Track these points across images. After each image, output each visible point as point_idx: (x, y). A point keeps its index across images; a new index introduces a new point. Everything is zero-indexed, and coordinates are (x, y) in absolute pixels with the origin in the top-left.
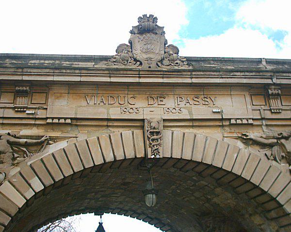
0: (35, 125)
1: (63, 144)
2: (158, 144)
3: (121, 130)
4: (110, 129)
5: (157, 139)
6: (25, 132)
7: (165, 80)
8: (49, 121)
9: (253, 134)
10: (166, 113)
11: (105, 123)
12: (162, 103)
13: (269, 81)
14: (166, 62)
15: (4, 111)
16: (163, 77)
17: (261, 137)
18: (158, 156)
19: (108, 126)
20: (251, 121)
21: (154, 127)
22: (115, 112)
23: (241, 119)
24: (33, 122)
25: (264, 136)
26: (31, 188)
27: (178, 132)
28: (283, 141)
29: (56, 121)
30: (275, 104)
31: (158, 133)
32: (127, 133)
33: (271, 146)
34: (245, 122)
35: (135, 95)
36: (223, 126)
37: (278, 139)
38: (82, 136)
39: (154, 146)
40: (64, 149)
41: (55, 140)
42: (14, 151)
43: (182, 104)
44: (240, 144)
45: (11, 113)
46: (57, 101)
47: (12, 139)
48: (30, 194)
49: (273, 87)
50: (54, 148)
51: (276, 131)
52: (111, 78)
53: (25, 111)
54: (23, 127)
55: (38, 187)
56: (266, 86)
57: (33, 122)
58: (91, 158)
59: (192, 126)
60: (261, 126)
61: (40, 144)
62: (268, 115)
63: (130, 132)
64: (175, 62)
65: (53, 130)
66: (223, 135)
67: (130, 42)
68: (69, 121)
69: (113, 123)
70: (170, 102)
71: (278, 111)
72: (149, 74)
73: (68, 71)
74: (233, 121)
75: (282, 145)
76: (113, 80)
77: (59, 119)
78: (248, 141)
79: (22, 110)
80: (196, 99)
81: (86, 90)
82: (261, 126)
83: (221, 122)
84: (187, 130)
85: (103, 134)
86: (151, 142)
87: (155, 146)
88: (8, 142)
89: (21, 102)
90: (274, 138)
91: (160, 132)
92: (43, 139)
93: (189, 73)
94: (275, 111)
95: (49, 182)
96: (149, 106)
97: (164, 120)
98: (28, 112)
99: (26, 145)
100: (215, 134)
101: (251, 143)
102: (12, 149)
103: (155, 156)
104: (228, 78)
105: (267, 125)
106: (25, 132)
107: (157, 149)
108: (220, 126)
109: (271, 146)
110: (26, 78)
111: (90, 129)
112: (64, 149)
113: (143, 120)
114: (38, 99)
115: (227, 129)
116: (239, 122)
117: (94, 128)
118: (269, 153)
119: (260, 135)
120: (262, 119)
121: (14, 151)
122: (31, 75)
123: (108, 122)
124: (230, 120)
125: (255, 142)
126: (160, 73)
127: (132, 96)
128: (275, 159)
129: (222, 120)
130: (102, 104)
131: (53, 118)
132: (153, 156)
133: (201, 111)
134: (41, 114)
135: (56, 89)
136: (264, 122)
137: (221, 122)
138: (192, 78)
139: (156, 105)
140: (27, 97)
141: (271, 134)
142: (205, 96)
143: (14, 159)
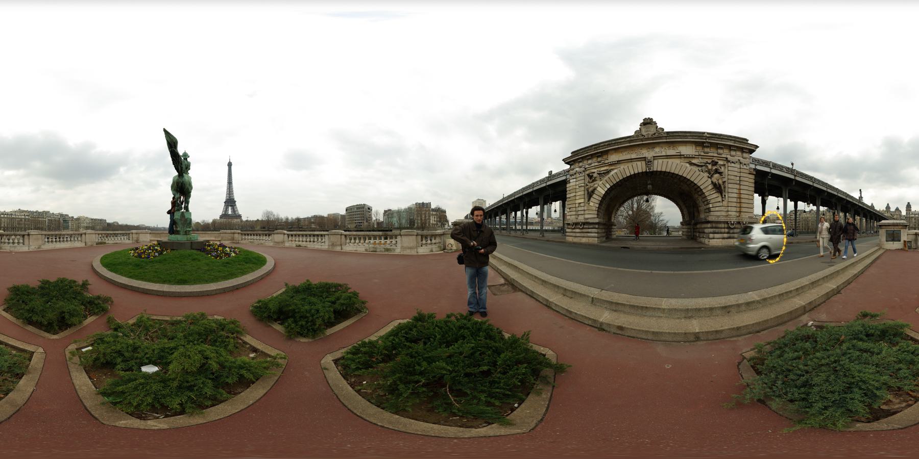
1: (615, 171)
9: (694, 161)
14: (657, 134)
19: (631, 162)
22: (634, 156)
24: (604, 165)
28: (708, 165)
33: (702, 166)
34: (691, 156)
36: (681, 158)
37: (705, 163)
38: (622, 166)
41: (613, 170)
42: (600, 176)
43: (662, 150)
44: (688, 165)
45: (597, 164)
47: (599, 172)
48: (606, 189)
50: (613, 173)
51: (705, 161)
55: (608, 186)
57: (604, 165)
59: (667, 158)
61: (608, 172)
62: (702, 154)
67: (640, 129)
70: (657, 149)
74: (685, 156)
75: (707, 166)
78: (691, 164)
79: (599, 162)
83: (680, 156)
84: (664, 160)
89: (599, 159)
90: (704, 163)
95: (612, 184)
99: (603, 173)
100: (677, 161)
109: (702, 166)
114: (605, 157)
115: (683, 159)
116: (688, 156)
118: (700, 169)
120: (699, 155)
121: (600, 176)
124: (684, 155)
125: (695, 164)
128: (702, 171)
129: (681, 155)
133: (671, 152)
134: (606, 162)
135: (610, 152)
136: (700, 157)
137: (680, 156)
141: (703, 161)
143: (600, 178)
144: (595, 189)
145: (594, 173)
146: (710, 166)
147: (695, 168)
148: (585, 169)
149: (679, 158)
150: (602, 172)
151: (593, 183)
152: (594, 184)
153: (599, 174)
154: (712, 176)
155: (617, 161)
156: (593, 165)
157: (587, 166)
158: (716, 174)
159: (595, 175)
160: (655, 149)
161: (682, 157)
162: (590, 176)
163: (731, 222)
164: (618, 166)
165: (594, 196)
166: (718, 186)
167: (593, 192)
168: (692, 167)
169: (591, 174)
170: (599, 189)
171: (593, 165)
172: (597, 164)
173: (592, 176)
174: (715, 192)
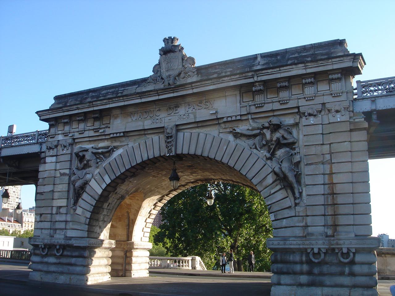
0: (105, 139)
1: (120, 151)
2: (171, 145)
3: (153, 136)
4: (147, 136)
5: (171, 142)
6: (101, 144)
7: (175, 94)
8: (112, 136)
9: (242, 128)
10: (179, 119)
11: (143, 133)
12: (177, 112)
13: (251, 80)
15: (89, 132)
16: (173, 92)
17: (248, 129)
18: (171, 154)
19: (145, 134)
20: (239, 118)
21: (169, 133)
23: (231, 117)
24: (104, 137)
25: (250, 128)
26: (105, 182)
27: (187, 133)
29: (115, 135)
30: (259, 99)
31: (171, 137)
32: (155, 138)
33: (255, 136)
34: (234, 118)
35: (160, 108)
36: (219, 124)
37: (261, 129)
38: (131, 143)
39: (169, 147)
40: (120, 154)
41: (116, 148)
42: (97, 158)
43: (190, 111)
44: (231, 138)
45: (92, 133)
46: (115, 120)
47: (95, 151)
48: (104, 186)
49: (257, 84)
50: (116, 154)
52: (142, 99)
53: (99, 131)
54: (100, 141)
56: (252, 84)
57: (104, 137)
58: (135, 159)
59: (198, 127)
60: (248, 119)
61: (110, 151)
62: (253, 109)
63: (158, 137)
64: (188, 74)
65: (115, 141)
66: (219, 131)
68: (122, 134)
69: (147, 132)
71: (261, 105)
72: (164, 91)
73: (116, 99)
76: (143, 100)
77: (117, 133)
78: (237, 135)
80: (200, 105)
81: (131, 110)
82: (248, 119)
84: (194, 131)
85: (142, 140)
86: (167, 144)
87: (170, 147)
88: (92, 152)
91: (172, 136)
92: (110, 148)
93: (190, 86)
94: (259, 105)
95: (113, 177)
96: (169, 115)
97: (177, 126)
98: (100, 131)
99: (102, 153)
100: (213, 131)
101: (239, 135)
102: (96, 157)
103: (170, 154)
104: (219, 83)
105: (252, 119)
106: (101, 144)
107: (171, 149)
108: (216, 124)
109: (255, 136)
110: (96, 108)
111: (135, 137)
112: (120, 154)
113: (164, 127)
115: (223, 125)
116: (229, 119)
117: (138, 137)
118: (251, 142)
119: (246, 128)
120: (248, 114)
121: (97, 158)
122: (97, 106)
123: (143, 132)
125: (242, 135)
126: (170, 90)
127: (158, 109)
128: (256, 148)
129: (218, 119)
130: (140, 119)
131: (113, 134)
132: (169, 154)
134: (108, 131)
135: (115, 112)
136: (250, 117)
137: (217, 121)
138: (193, 89)
139: (173, 114)
140: (99, 120)
141: (255, 125)
142: (207, 101)
143: (97, 163)
144: (86, 183)
145: (87, 150)
146: (268, 134)
147: (244, 143)
148: (74, 139)
149: (216, 124)
150: (100, 151)
151: (84, 171)
152: (86, 174)
153: (95, 154)
154: (273, 154)
155: (123, 132)
156: (86, 134)
157: (77, 135)
158: (280, 148)
159: (88, 156)
160: (179, 109)
161: (221, 121)
162: (81, 158)
163: (313, 249)
164: (125, 141)
165: (85, 196)
166: (282, 176)
167: (83, 188)
168: (238, 141)
169: (81, 154)
170: (93, 183)
171: (86, 134)
172: (92, 133)
173: (84, 156)
174: (278, 187)
